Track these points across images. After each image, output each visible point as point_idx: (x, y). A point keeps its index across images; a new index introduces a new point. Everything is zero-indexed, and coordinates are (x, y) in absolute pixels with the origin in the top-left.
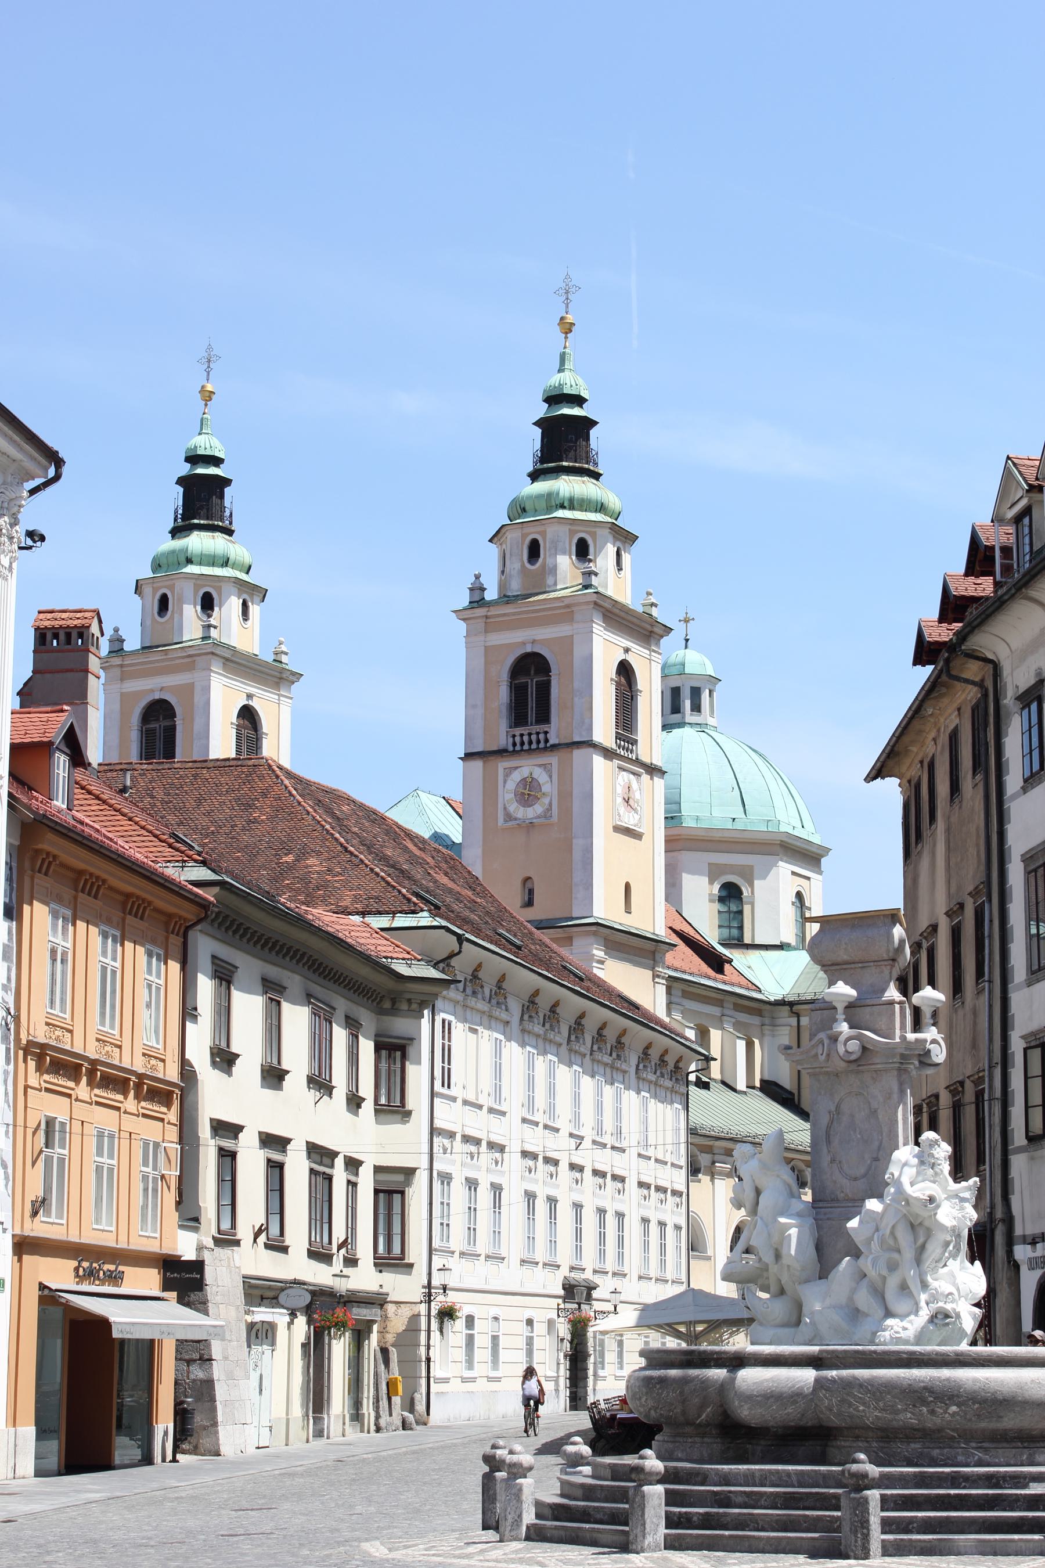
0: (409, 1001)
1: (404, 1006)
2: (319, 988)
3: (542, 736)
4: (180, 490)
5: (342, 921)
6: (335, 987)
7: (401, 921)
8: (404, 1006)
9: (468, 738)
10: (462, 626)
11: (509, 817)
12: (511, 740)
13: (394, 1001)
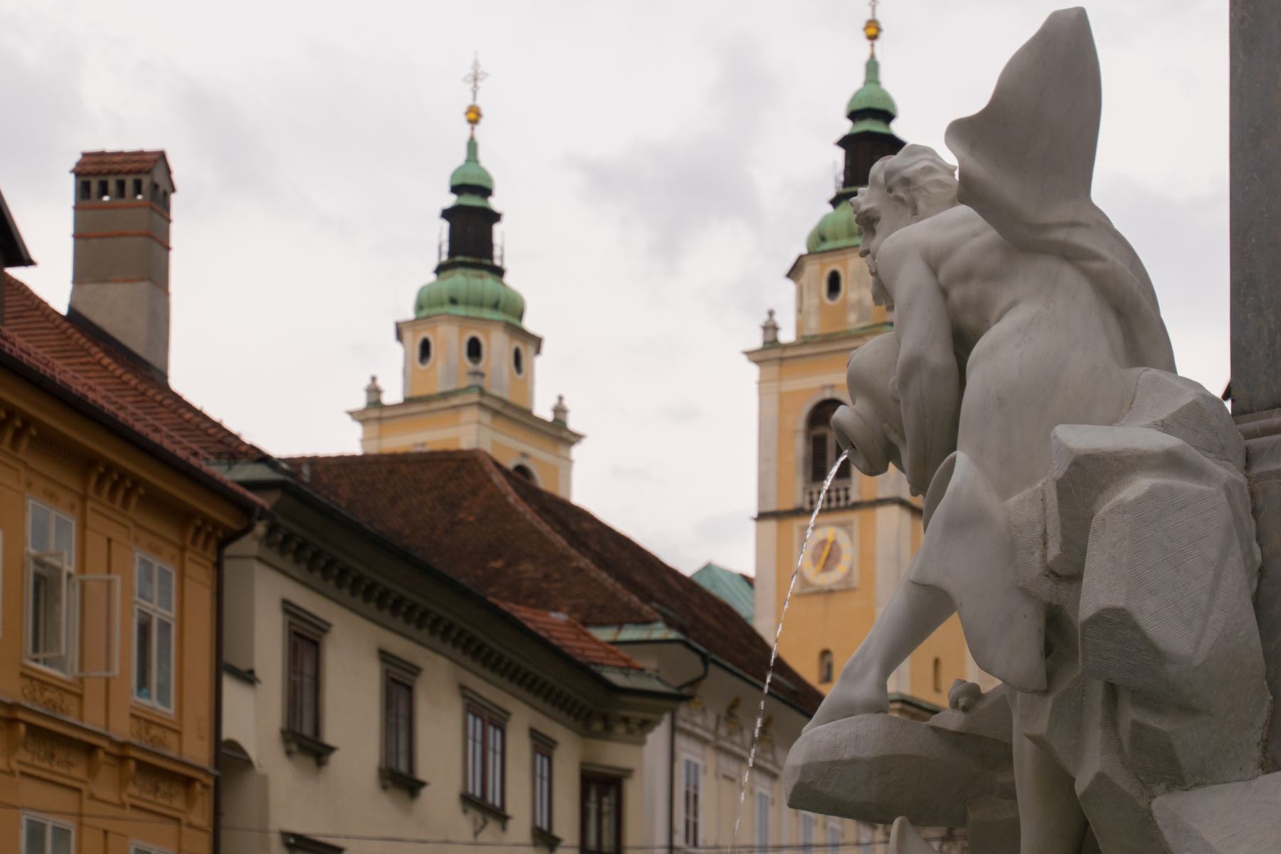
0: (626, 720)
1: (620, 729)
2: (482, 683)
3: (842, 494)
4: (445, 225)
5: (539, 618)
6: (513, 687)
7: (630, 633)
8: (620, 729)
9: (762, 496)
10: (753, 371)
11: (804, 582)
12: (807, 498)
13: (605, 719)
